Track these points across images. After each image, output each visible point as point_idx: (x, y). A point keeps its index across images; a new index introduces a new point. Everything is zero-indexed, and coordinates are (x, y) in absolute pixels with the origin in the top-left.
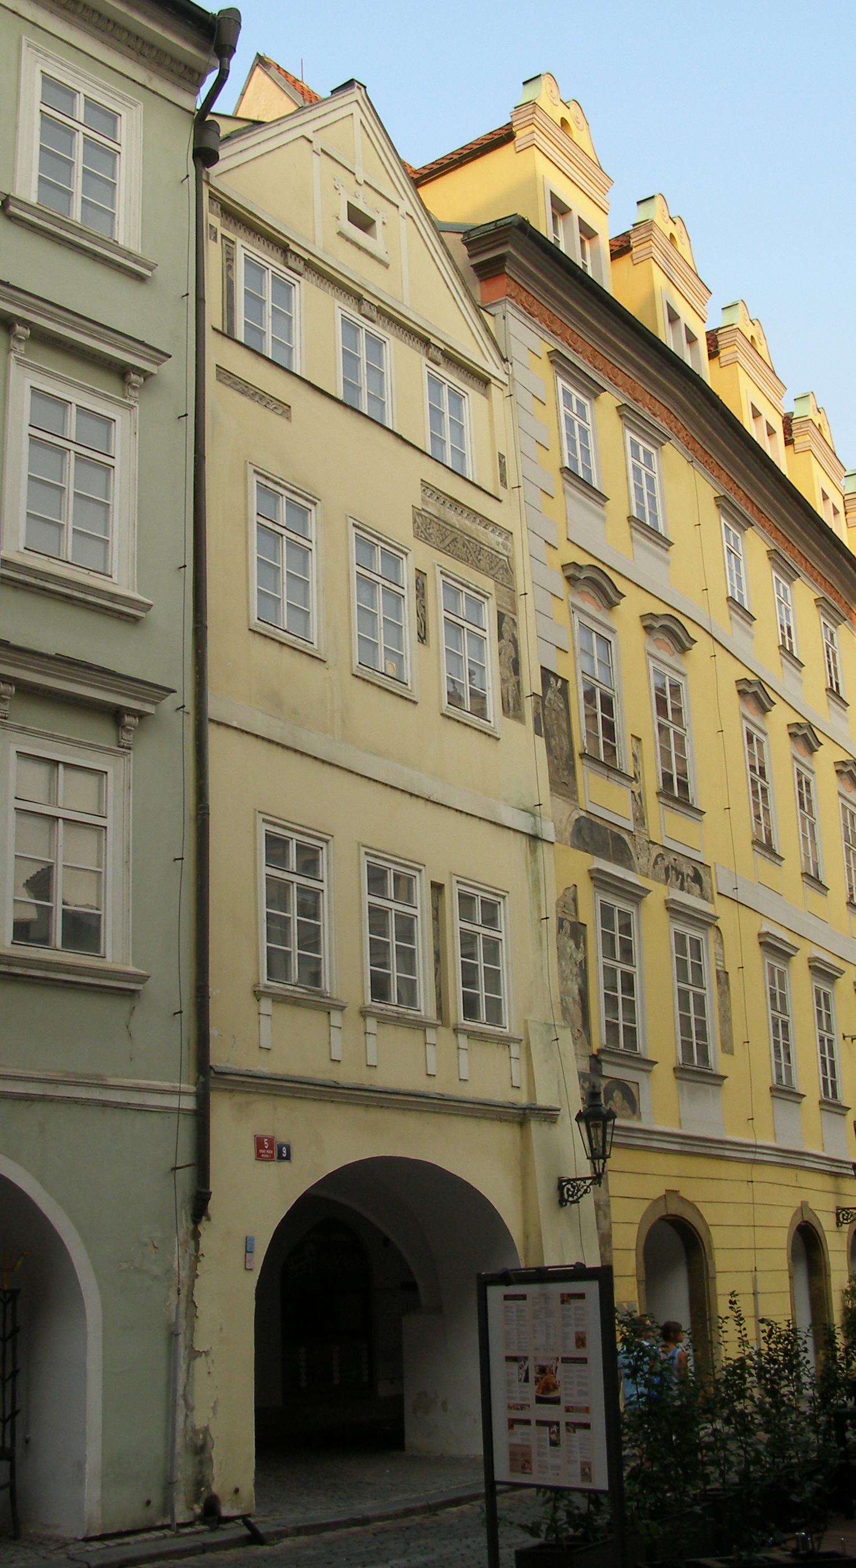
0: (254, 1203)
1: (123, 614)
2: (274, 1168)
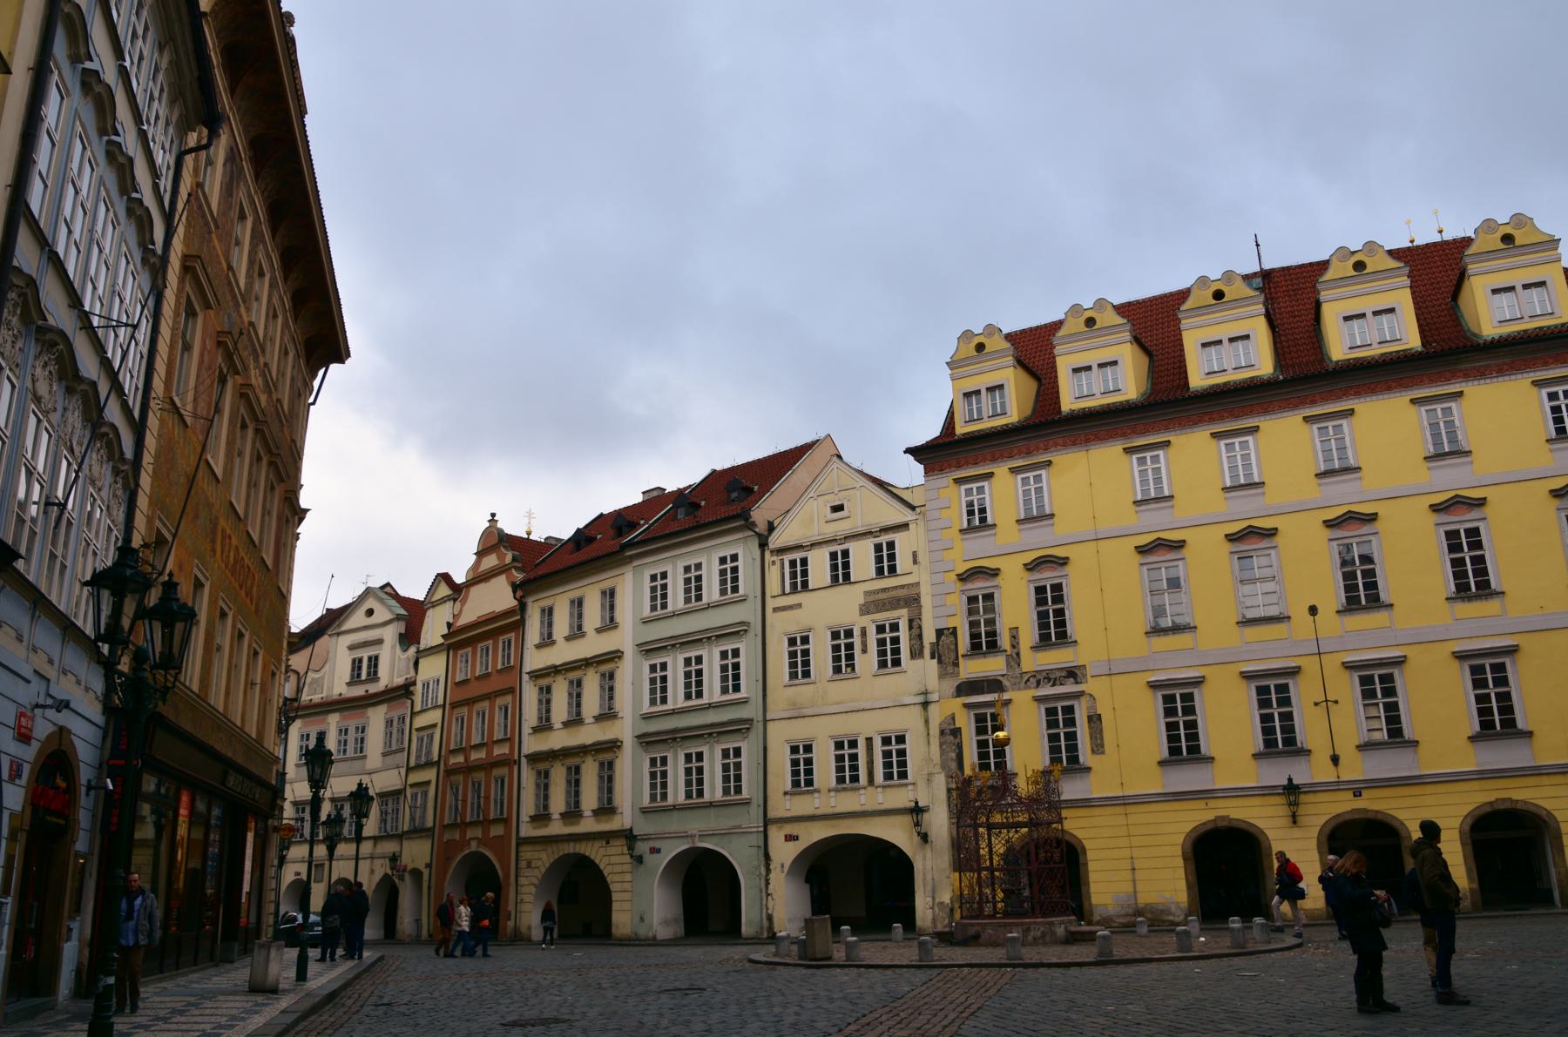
0: (784, 853)
1: (745, 701)
2: (791, 844)
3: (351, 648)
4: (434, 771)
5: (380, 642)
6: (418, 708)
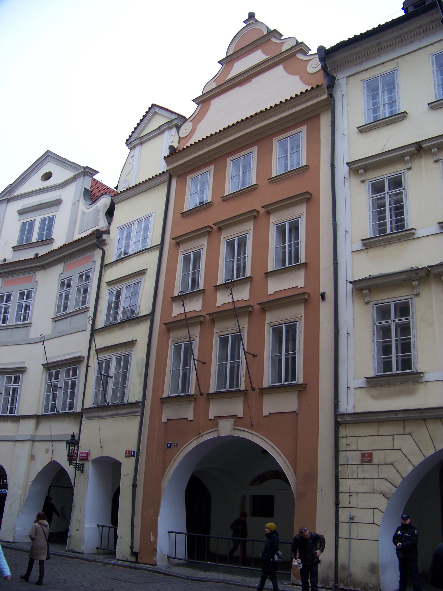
3: (21, 213)
4: (144, 327)
5: (58, 203)
6: (110, 259)
